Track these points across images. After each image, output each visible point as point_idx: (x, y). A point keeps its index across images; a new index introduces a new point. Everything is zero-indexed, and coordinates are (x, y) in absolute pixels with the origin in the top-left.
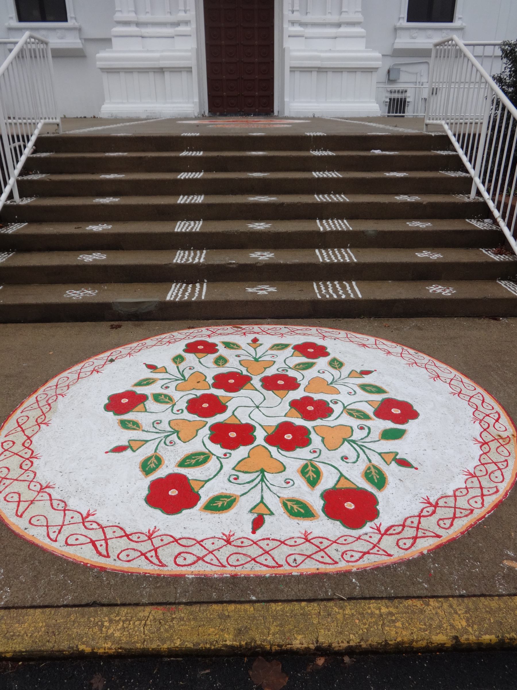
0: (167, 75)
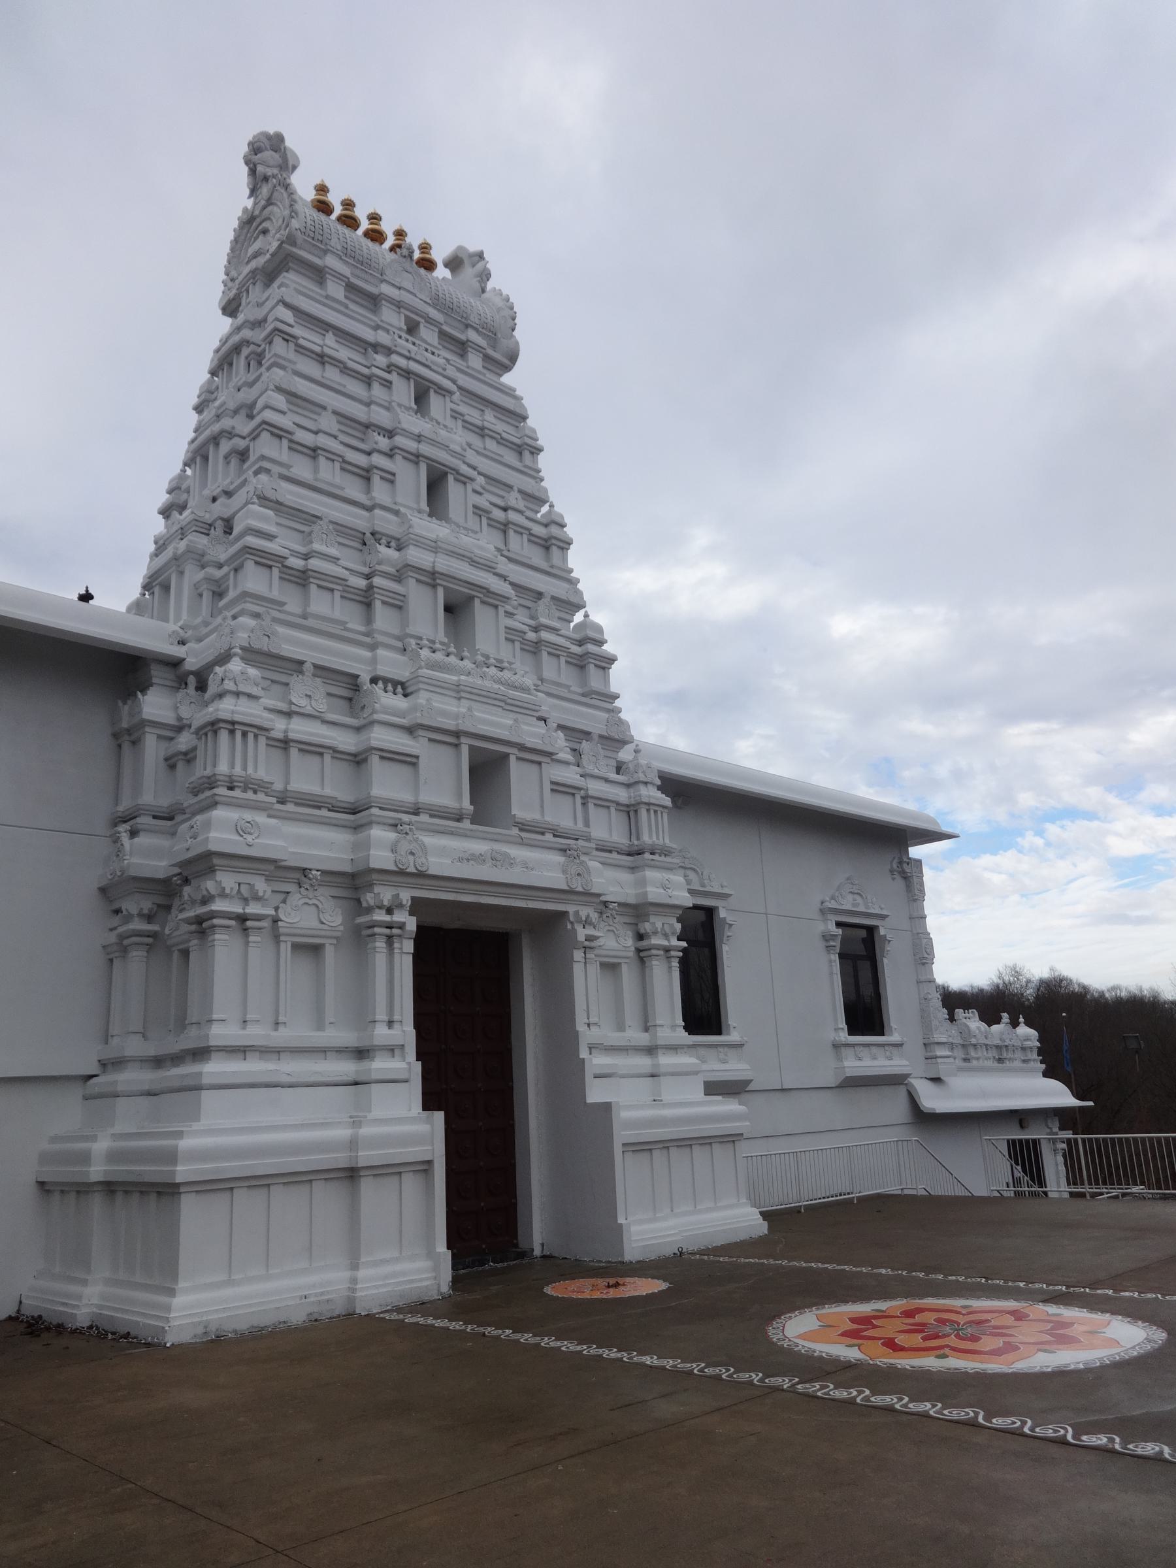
0: (367, 1186)
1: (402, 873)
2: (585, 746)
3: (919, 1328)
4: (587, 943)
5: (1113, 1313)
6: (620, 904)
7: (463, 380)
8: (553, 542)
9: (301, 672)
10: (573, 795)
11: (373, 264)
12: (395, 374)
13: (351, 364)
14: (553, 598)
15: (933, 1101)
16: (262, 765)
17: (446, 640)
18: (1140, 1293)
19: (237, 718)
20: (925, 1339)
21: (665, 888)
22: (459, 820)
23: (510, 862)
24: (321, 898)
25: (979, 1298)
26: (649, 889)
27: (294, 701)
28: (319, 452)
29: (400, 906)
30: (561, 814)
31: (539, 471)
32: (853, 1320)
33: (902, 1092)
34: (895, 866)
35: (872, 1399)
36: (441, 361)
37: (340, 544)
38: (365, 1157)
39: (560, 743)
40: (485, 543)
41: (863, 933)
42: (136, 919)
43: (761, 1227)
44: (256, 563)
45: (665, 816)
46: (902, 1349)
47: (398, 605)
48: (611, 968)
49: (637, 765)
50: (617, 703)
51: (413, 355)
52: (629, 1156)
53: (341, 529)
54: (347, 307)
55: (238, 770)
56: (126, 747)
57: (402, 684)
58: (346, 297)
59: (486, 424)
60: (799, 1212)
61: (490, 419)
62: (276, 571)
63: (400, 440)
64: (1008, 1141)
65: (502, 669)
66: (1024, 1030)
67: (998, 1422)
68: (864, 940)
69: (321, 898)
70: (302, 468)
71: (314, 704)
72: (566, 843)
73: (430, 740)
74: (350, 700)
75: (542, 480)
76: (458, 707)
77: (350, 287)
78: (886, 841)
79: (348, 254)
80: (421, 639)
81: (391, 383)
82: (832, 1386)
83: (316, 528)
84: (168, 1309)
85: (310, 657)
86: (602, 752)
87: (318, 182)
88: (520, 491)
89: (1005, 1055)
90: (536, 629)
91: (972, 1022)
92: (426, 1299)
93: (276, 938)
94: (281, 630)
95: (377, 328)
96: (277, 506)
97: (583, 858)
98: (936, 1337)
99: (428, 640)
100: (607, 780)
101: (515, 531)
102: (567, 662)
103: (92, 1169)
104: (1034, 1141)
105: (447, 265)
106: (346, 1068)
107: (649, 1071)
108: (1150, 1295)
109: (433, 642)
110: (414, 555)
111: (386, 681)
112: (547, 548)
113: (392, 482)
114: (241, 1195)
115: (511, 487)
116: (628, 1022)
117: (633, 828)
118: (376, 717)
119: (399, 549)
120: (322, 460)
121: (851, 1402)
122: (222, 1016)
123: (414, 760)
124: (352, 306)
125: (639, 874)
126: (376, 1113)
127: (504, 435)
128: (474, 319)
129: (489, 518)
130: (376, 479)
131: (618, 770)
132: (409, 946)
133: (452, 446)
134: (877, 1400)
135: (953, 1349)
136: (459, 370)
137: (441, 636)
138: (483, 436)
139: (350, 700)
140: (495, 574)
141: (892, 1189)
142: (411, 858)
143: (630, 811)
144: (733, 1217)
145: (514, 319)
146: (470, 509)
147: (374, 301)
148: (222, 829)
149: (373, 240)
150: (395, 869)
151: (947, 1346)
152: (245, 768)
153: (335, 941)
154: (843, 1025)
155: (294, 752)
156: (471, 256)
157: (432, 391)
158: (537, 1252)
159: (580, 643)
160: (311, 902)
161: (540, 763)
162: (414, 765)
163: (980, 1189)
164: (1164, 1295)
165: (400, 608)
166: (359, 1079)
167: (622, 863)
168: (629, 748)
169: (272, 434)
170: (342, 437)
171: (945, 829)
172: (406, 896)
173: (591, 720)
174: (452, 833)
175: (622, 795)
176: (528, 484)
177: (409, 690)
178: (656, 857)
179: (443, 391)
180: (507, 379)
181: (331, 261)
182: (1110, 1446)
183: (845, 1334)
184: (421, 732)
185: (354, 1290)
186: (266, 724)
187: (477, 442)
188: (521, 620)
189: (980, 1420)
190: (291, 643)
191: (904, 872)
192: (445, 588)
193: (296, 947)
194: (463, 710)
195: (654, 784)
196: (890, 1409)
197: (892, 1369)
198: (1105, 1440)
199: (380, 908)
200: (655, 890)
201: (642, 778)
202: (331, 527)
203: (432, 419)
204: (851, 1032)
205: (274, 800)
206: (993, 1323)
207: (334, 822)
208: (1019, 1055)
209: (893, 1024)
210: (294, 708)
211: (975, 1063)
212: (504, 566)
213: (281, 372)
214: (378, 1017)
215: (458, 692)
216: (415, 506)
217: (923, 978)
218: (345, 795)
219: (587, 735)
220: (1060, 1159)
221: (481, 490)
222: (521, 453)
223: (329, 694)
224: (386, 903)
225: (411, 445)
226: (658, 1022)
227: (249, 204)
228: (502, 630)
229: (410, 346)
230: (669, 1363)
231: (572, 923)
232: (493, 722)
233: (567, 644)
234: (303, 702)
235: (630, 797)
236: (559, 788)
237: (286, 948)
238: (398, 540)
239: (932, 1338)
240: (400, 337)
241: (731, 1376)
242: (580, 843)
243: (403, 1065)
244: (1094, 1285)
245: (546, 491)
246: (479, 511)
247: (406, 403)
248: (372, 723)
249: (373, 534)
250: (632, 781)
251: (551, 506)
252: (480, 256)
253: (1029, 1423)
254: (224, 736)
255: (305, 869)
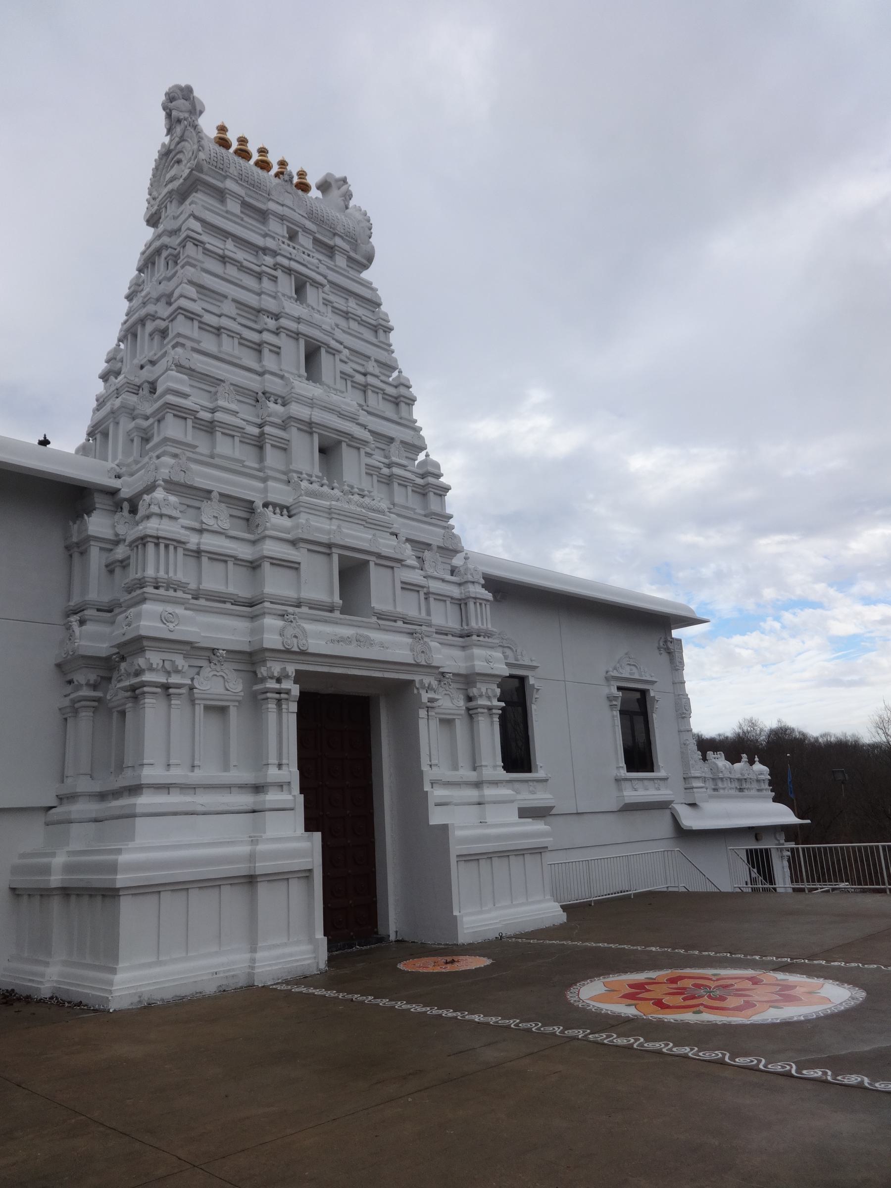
0: (262, 889)
1: (288, 652)
2: (427, 555)
3: (680, 992)
4: (429, 704)
5: (826, 978)
6: (454, 674)
7: (332, 276)
8: (401, 399)
9: (210, 499)
10: (418, 591)
11: (262, 187)
12: (279, 271)
13: (245, 263)
14: (402, 442)
15: (691, 820)
16: (181, 570)
17: (320, 474)
18: (846, 963)
19: (161, 534)
20: (684, 999)
21: (488, 662)
22: (331, 611)
23: (370, 643)
24: (226, 671)
25: (725, 968)
26: (477, 663)
27: (204, 521)
28: (222, 330)
29: (287, 677)
30: (409, 606)
31: (390, 345)
32: (631, 986)
33: (667, 813)
34: (661, 644)
35: (646, 1045)
36: (315, 261)
37: (239, 401)
38: (262, 867)
39: (408, 552)
40: (350, 400)
41: (638, 695)
42: (85, 688)
43: (562, 917)
44: (175, 415)
45: (488, 606)
46: (668, 1007)
47: (284, 448)
48: (447, 722)
49: (467, 569)
50: (451, 522)
51: (293, 257)
52: (462, 864)
53: (240, 390)
54: (242, 220)
55: (162, 574)
56: (76, 556)
57: (287, 508)
58: (242, 212)
59: (350, 310)
60: (590, 905)
61: (352, 305)
62: (189, 422)
63: (284, 322)
64: (747, 850)
65: (363, 496)
66: (758, 767)
67: (740, 1061)
68: (638, 700)
69: (226, 671)
70: (209, 343)
71: (219, 522)
72: (413, 628)
73: (309, 550)
74: (248, 520)
75: (393, 352)
76: (330, 525)
77: (245, 204)
78: (655, 626)
79: (242, 179)
80: (301, 473)
81: (276, 278)
82: (615, 1036)
83: (220, 389)
84: (111, 983)
85: (217, 487)
86: (440, 559)
87: (219, 123)
88: (376, 361)
89: (744, 786)
90: (389, 466)
91: (720, 761)
92: (308, 973)
93: (192, 702)
94: (194, 467)
95: (265, 236)
96: (191, 372)
97: (426, 639)
98: (693, 997)
99: (307, 474)
100: (443, 580)
101: (373, 391)
102: (413, 491)
103: (52, 878)
104: (766, 850)
105: (319, 187)
106: (246, 800)
107: (476, 800)
108: (853, 965)
109: (311, 476)
110: (297, 410)
111: (275, 505)
112: (397, 404)
113: (278, 354)
114: (166, 897)
115: (369, 358)
116: (460, 764)
117: (464, 617)
118: (267, 533)
119: (284, 405)
120: (224, 336)
121: (630, 1047)
122: (151, 761)
123: (296, 566)
124: (246, 219)
125: (468, 652)
126: (269, 834)
127: (364, 318)
128: (340, 229)
129: (352, 381)
130: (266, 352)
131: (452, 573)
132: (294, 707)
133: (324, 326)
134: (650, 1046)
135: (706, 1007)
136: (328, 268)
137: (317, 471)
138: (347, 319)
139: (248, 520)
140: (358, 424)
141: (660, 887)
142: (295, 640)
143: (461, 604)
144: (540, 910)
145: (370, 229)
146: (338, 375)
147: (263, 215)
148: (150, 619)
149: (262, 168)
150: (283, 648)
151: (702, 1004)
152: (167, 573)
153: (237, 704)
154: (623, 764)
155: (204, 560)
156: (337, 180)
157: (308, 284)
158: (392, 937)
159: (423, 476)
160: (218, 674)
161: (392, 568)
162: (297, 569)
163: (726, 887)
164: (863, 965)
165: (285, 450)
166: (256, 808)
167: (455, 643)
168: (461, 556)
169: (186, 317)
170: (240, 319)
171: (699, 615)
172: (291, 669)
173: (432, 534)
174: (326, 621)
175: (455, 592)
176: (382, 355)
177: (293, 512)
178: (481, 638)
179: (317, 284)
180: (366, 275)
181: (230, 184)
182: (824, 1078)
183: (626, 996)
184: (302, 545)
185: (253, 968)
186: (183, 539)
187: (343, 323)
188: (378, 459)
189: (727, 1059)
190: (202, 476)
191: (668, 648)
192: (320, 434)
193: (207, 708)
194: (334, 527)
195: (479, 583)
196: (659, 1053)
197: (661, 1022)
198: (820, 1073)
199: (271, 678)
200: (482, 663)
201: (470, 578)
202: (232, 388)
203: (308, 306)
204: (629, 769)
205: (190, 596)
206: (736, 986)
207: (238, 613)
208: (755, 785)
209: (661, 764)
210: (204, 526)
211: (722, 792)
212: (364, 418)
213: (192, 270)
214: (270, 761)
215: (330, 514)
216: (296, 372)
217: (682, 729)
218: (244, 592)
219: (428, 546)
220: (786, 863)
221: (346, 360)
222: (376, 332)
223: (231, 516)
224: (276, 674)
225: (293, 326)
226: (483, 763)
227: (167, 140)
228: (363, 467)
229: (291, 249)
230: (492, 1020)
231: (418, 689)
232: (358, 537)
233: (413, 477)
234: (212, 522)
235: (461, 593)
236: (407, 587)
237: (199, 710)
238: (283, 398)
239: (690, 998)
240: (283, 243)
241: (539, 1029)
242: (424, 628)
243: (290, 797)
244: (811, 957)
245: (396, 361)
246: (345, 376)
247: (288, 292)
248: (264, 537)
249: (264, 393)
250: (463, 581)
251: (400, 372)
252: (344, 181)
253: (763, 1061)
254: (151, 548)
255: (214, 649)
